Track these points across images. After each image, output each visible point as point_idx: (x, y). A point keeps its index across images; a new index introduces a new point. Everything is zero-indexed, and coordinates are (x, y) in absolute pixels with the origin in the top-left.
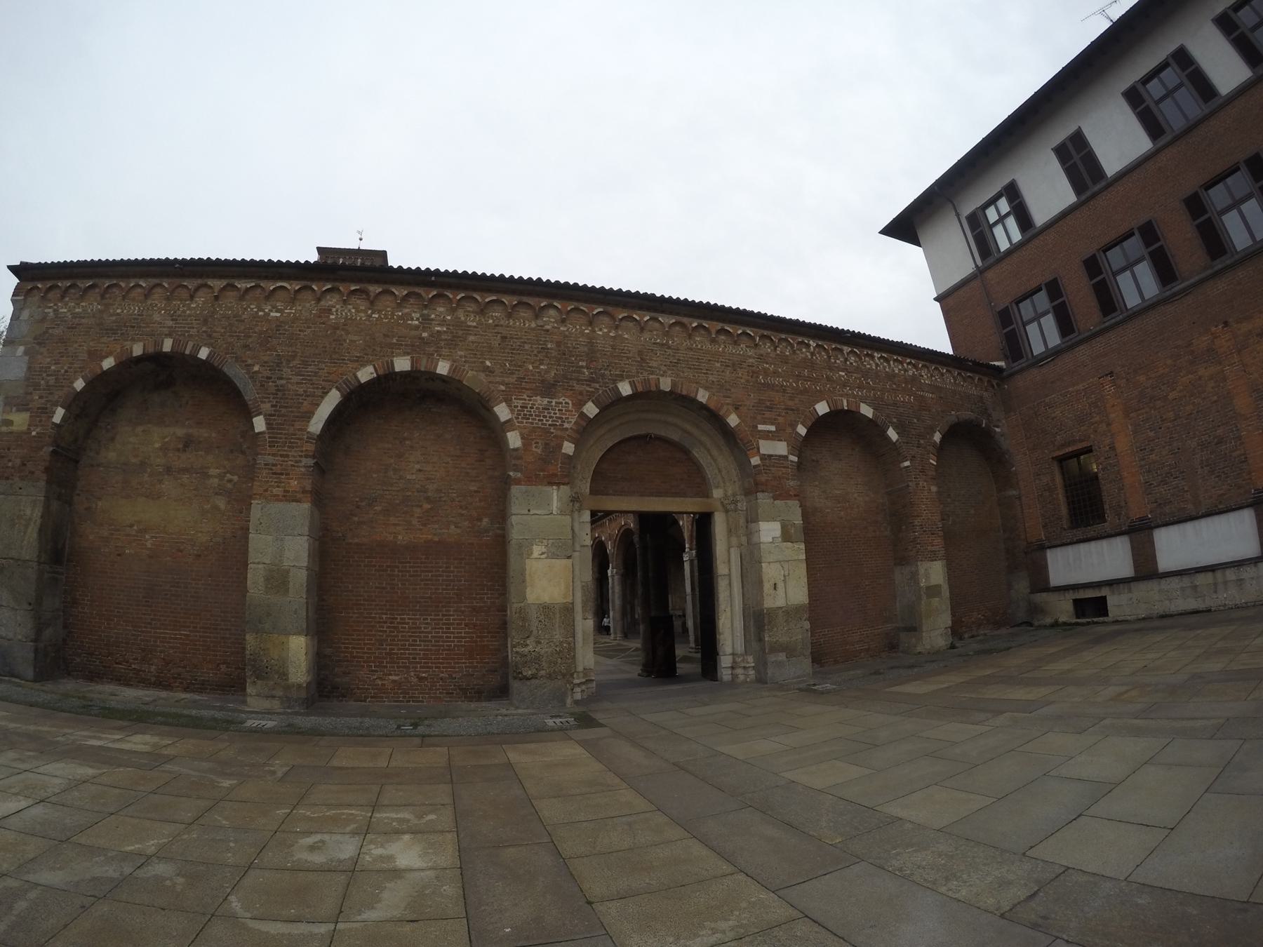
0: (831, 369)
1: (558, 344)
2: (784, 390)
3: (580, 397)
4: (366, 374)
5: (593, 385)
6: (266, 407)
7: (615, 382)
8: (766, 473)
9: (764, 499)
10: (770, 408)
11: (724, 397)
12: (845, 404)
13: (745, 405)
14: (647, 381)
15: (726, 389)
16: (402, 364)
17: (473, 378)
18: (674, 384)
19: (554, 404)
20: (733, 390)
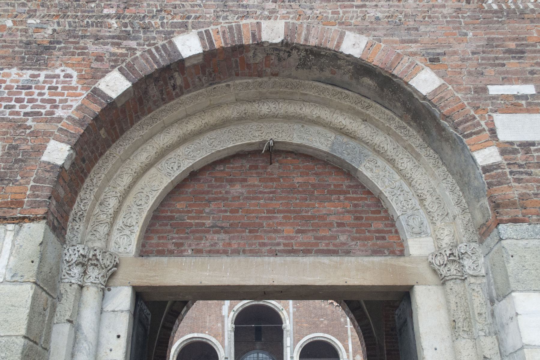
3: (95, 65)
5: (125, 43)
7: (169, 35)
8: (519, 181)
11: (403, 42)
13: (455, 53)
15: (409, 29)
18: (291, 30)
19: (42, 78)
20: (422, 28)
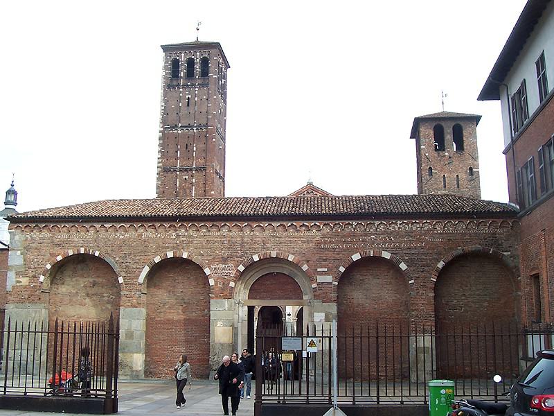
0: (366, 235)
1: (229, 241)
2: (334, 249)
4: (157, 259)
6: (123, 274)
9: (317, 303)
10: (325, 260)
12: (372, 253)
14: (265, 254)
16: (170, 255)
17: (196, 259)
